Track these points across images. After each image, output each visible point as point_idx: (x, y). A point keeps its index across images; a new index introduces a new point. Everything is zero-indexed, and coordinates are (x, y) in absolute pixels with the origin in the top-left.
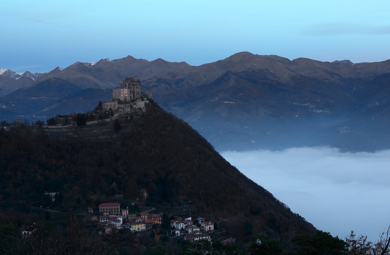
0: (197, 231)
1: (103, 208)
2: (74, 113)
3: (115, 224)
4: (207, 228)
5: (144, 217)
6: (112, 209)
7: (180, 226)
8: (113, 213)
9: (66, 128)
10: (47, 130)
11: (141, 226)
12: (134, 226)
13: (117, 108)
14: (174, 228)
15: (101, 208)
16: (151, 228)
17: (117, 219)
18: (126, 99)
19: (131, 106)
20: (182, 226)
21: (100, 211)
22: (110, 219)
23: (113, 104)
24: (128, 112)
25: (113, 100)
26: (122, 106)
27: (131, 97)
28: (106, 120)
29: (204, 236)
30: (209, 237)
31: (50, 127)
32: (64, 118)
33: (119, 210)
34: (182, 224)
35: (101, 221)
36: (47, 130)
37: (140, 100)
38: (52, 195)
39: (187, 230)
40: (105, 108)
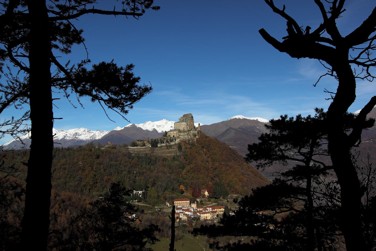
1: (177, 203)
2: (148, 138)
3: (188, 214)
5: (209, 209)
6: (184, 203)
8: (185, 206)
9: (143, 149)
13: (178, 136)
15: (176, 202)
16: (216, 217)
17: (190, 210)
18: (184, 129)
22: (183, 210)
23: (175, 132)
24: (186, 138)
27: (187, 128)
28: (171, 143)
31: (132, 148)
32: (142, 142)
33: (189, 204)
35: (177, 212)
37: (194, 130)
38: (138, 193)
40: (169, 136)
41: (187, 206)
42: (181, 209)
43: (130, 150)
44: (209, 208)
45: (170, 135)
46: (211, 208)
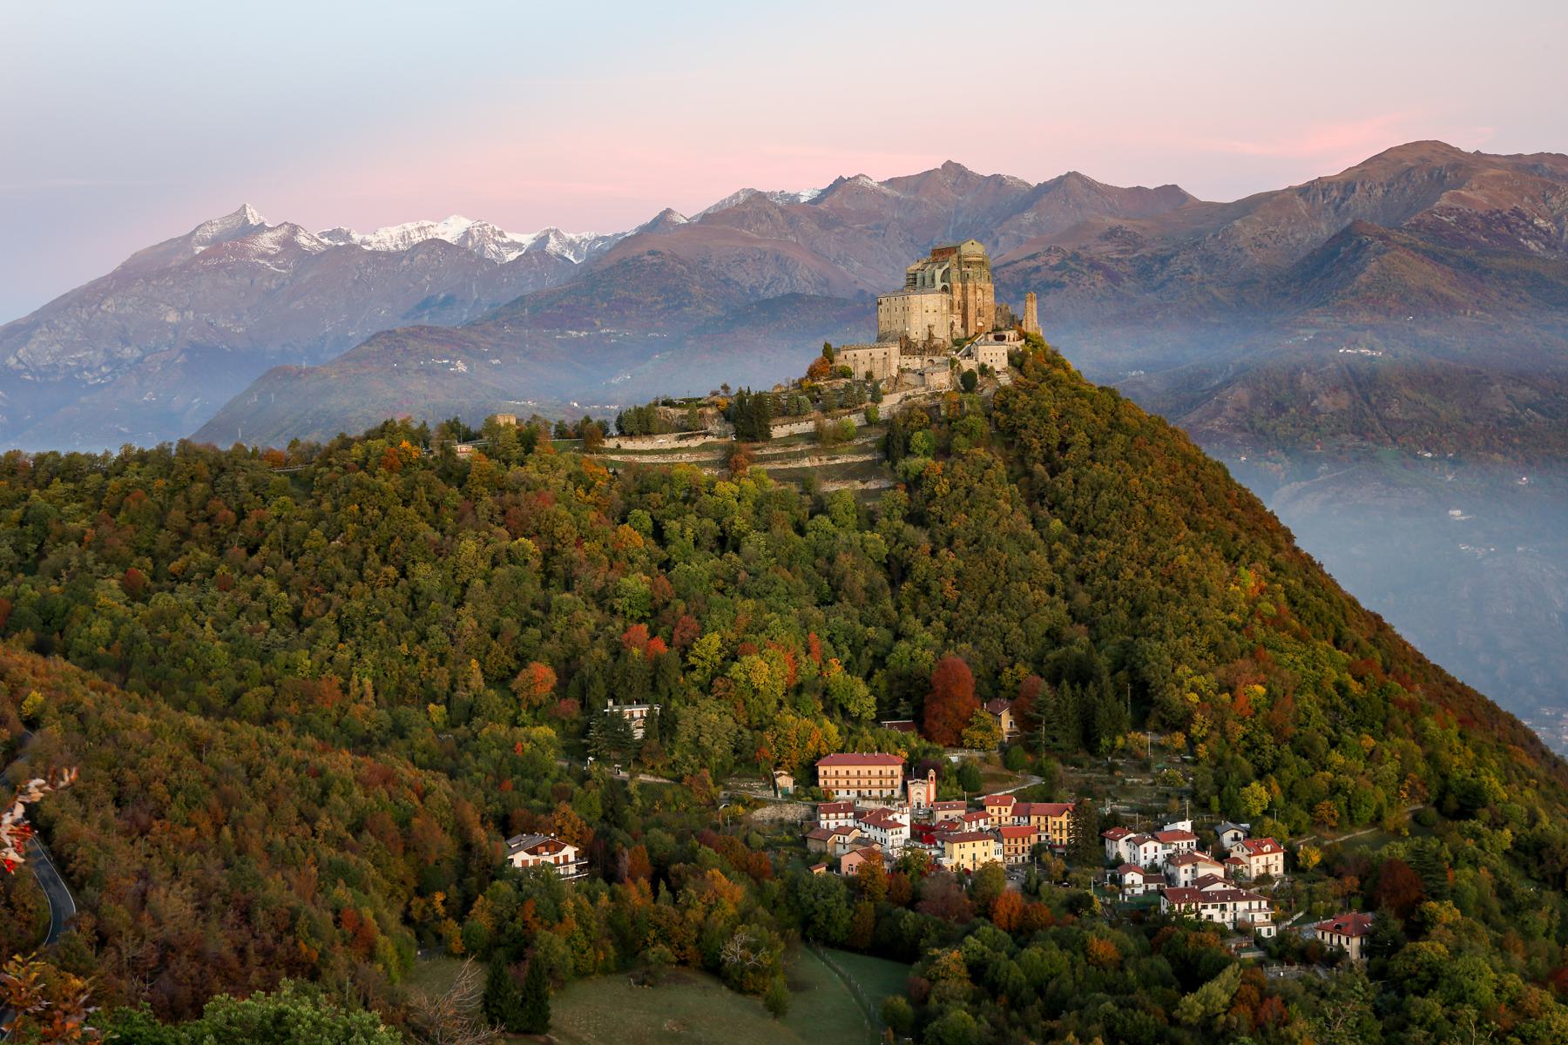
0: (1214, 880)
2: (725, 388)
4: (1256, 865)
7: (1142, 855)
8: (875, 793)
9: (688, 449)
10: (613, 457)
11: (985, 849)
12: (956, 846)
13: (895, 372)
14: (1119, 862)
18: (931, 336)
19: (953, 362)
20: (1150, 854)
21: (821, 782)
23: (878, 353)
25: (882, 339)
26: (916, 363)
29: (1243, 899)
30: (1264, 904)
31: (628, 445)
32: (686, 412)
33: (898, 782)
34: (1150, 845)
35: (823, 823)
36: (617, 458)
37: (991, 337)
39: (1171, 869)
40: (846, 373)
41: (886, 793)
42: (849, 807)
43: (613, 457)
44: (996, 809)
45: (851, 366)
46: (1010, 809)
